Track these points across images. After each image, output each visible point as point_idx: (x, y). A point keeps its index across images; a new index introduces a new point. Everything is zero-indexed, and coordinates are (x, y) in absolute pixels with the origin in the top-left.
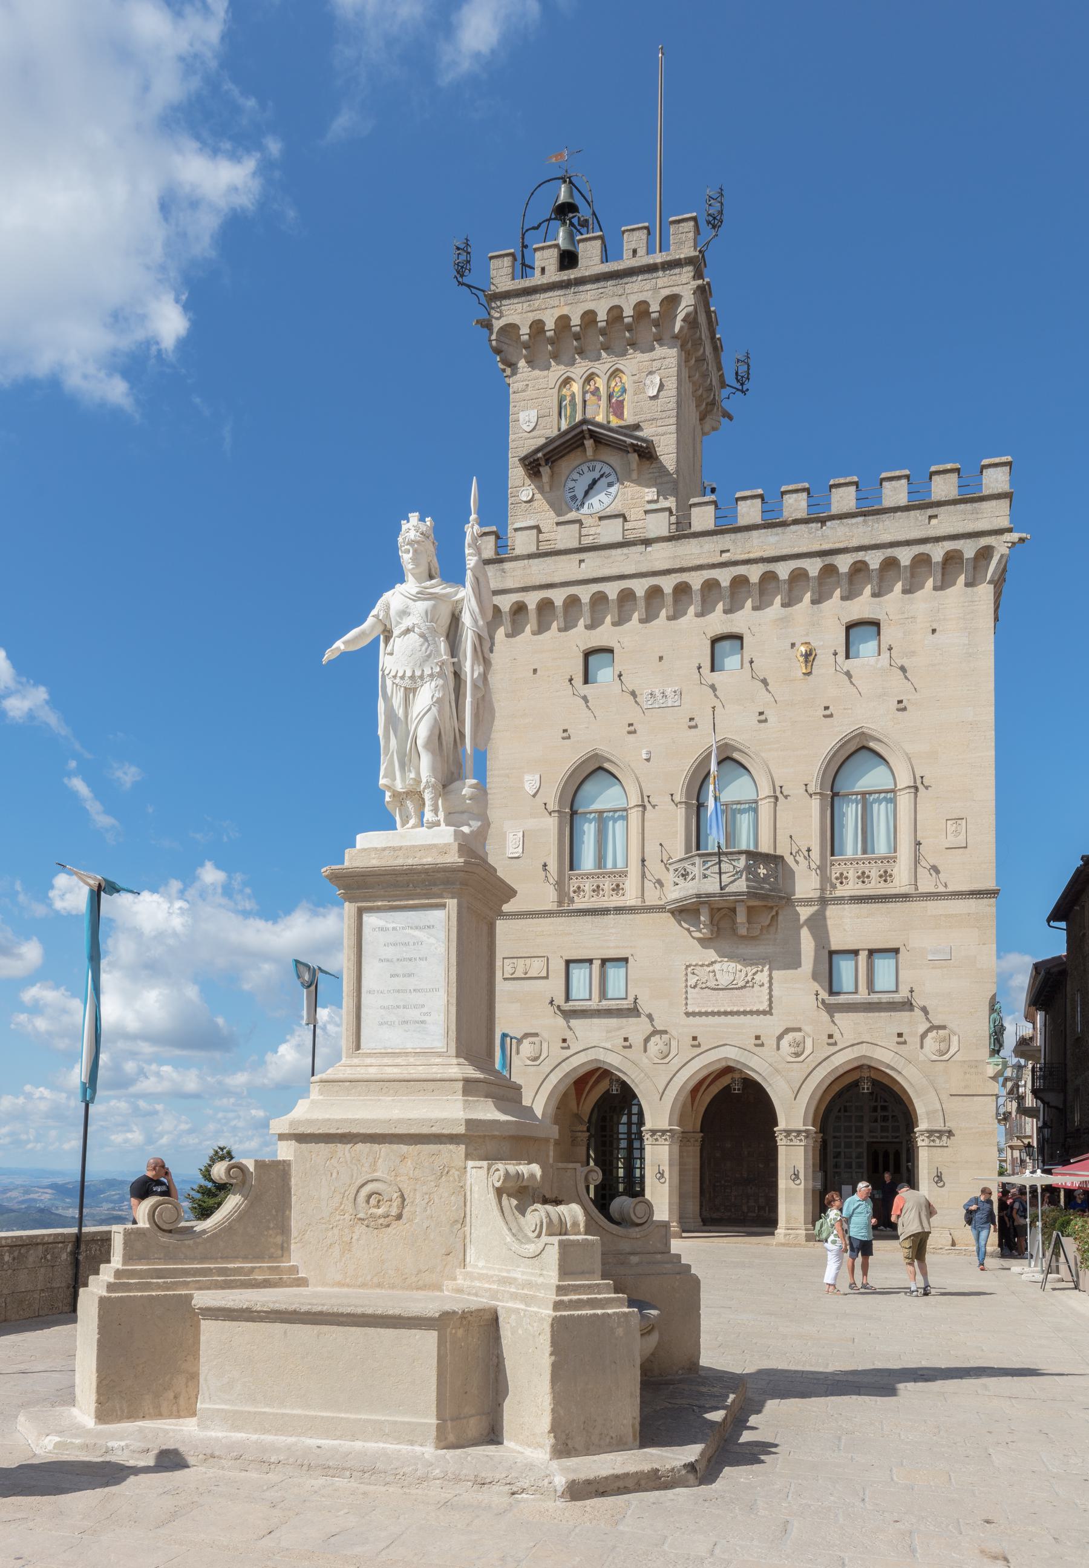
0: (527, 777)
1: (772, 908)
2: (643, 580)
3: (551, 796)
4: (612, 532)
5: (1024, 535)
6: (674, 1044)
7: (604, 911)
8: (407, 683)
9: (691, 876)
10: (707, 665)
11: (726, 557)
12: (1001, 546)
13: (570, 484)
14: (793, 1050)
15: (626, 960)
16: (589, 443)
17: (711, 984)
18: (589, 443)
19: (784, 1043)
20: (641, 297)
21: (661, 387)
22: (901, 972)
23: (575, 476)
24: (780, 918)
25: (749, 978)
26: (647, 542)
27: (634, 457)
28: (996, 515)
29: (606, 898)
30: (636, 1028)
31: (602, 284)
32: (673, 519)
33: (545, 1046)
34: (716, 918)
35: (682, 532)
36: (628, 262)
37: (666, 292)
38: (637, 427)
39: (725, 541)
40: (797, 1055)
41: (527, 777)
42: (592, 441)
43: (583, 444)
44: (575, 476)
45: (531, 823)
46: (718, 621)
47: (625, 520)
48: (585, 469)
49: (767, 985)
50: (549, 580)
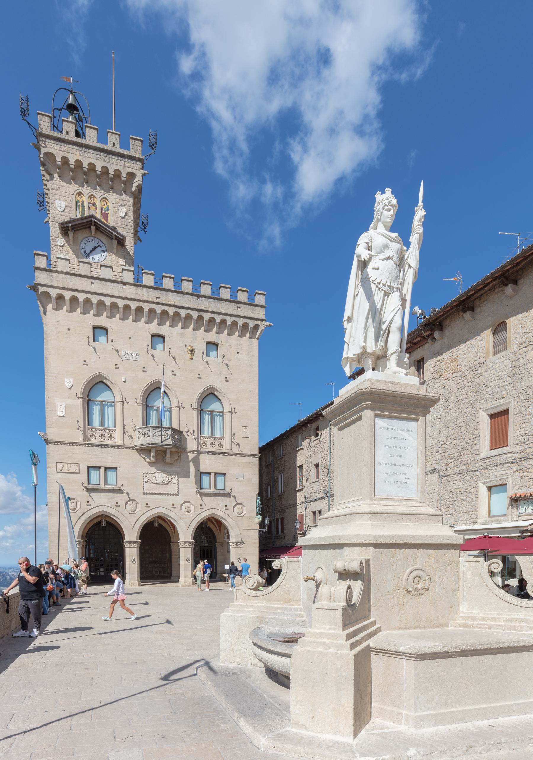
0: (66, 379)
1: (179, 452)
2: (122, 300)
3: (79, 390)
5: (271, 324)
6: (138, 505)
7: (106, 446)
10: (150, 345)
11: (158, 300)
12: (262, 326)
14: (187, 510)
15: (116, 468)
16: (93, 228)
17: (154, 481)
18: (93, 228)
19: (183, 507)
21: (126, 214)
22: (226, 482)
24: (181, 457)
27: (115, 242)
28: (260, 313)
29: (106, 440)
30: (121, 498)
33: (78, 504)
35: (138, 283)
37: (129, 170)
39: (159, 293)
40: (188, 512)
41: (66, 379)
42: (95, 227)
43: (90, 227)
45: (69, 401)
49: (177, 484)
50: (76, 288)
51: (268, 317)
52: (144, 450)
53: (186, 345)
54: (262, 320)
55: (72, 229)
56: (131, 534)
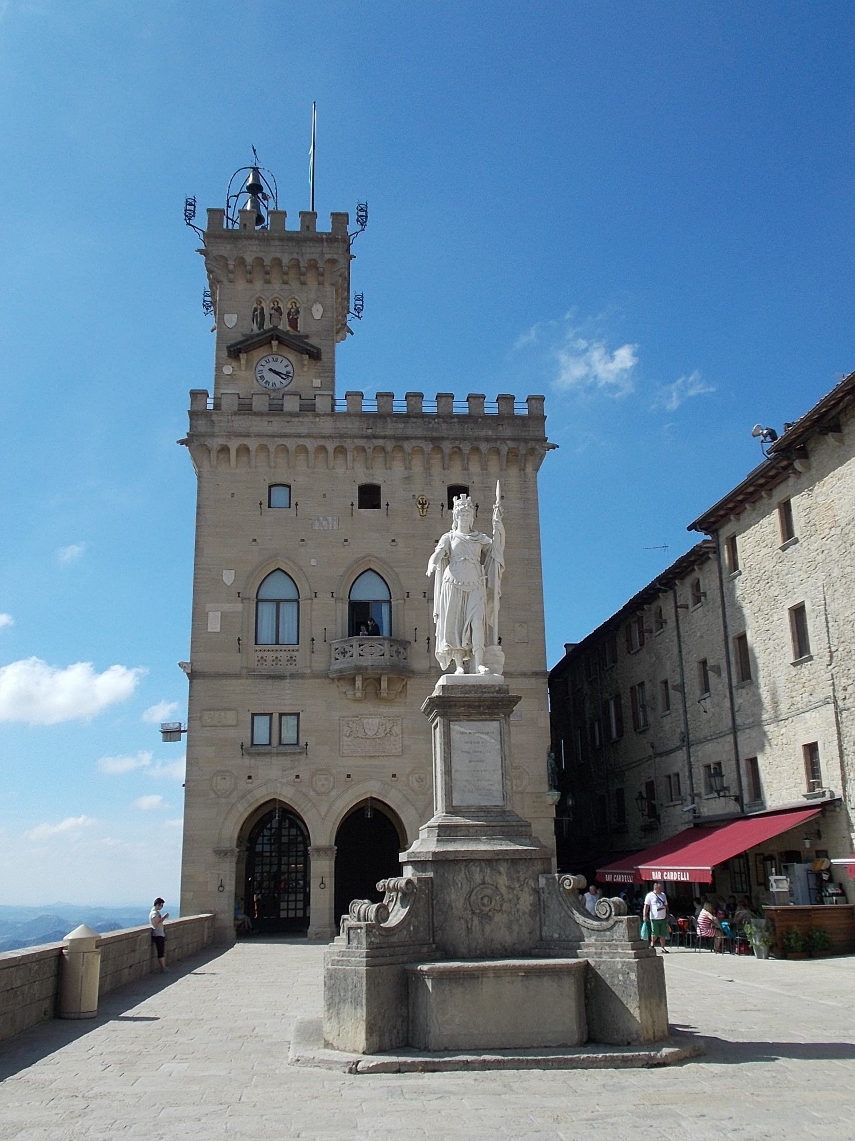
9: (349, 654)
16: (275, 343)
18: (275, 343)
20: (313, 256)
23: (264, 363)
25: (388, 730)
34: (365, 684)
38: (307, 337)
45: (227, 607)
48: (271, 360)
52: (347, 678)
56: (322, 832)
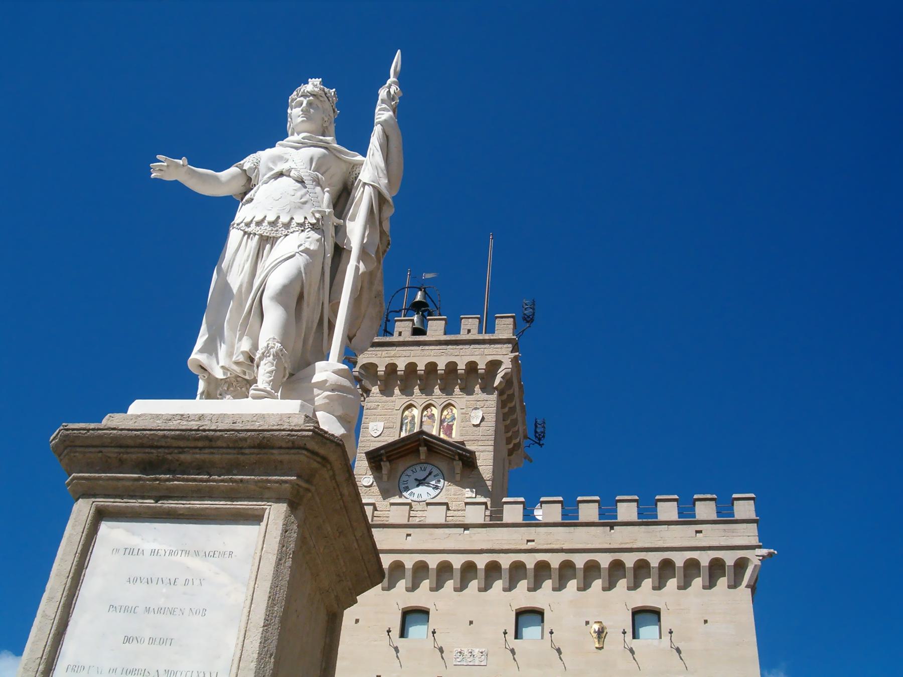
4: (436, 515)
5: (772, 550)
8: (265, 229)
11: (531, 545)
12: (755, 557)
13: (404, 478)
16: (423, 449)
18: (423, 449)
21: (483, 419)
26: (466, 527)
27: (458, 465)
31: (444, 347)
32: (488, 513)
36: (463, 336)
37: (490, 358)
43: (418, 451)
44: (409, 472)
46: (522, 597)
47: (448, 509)
51: (765, 540)
53: (587, 623)
54: (752, 548)
55: (388, 457)
